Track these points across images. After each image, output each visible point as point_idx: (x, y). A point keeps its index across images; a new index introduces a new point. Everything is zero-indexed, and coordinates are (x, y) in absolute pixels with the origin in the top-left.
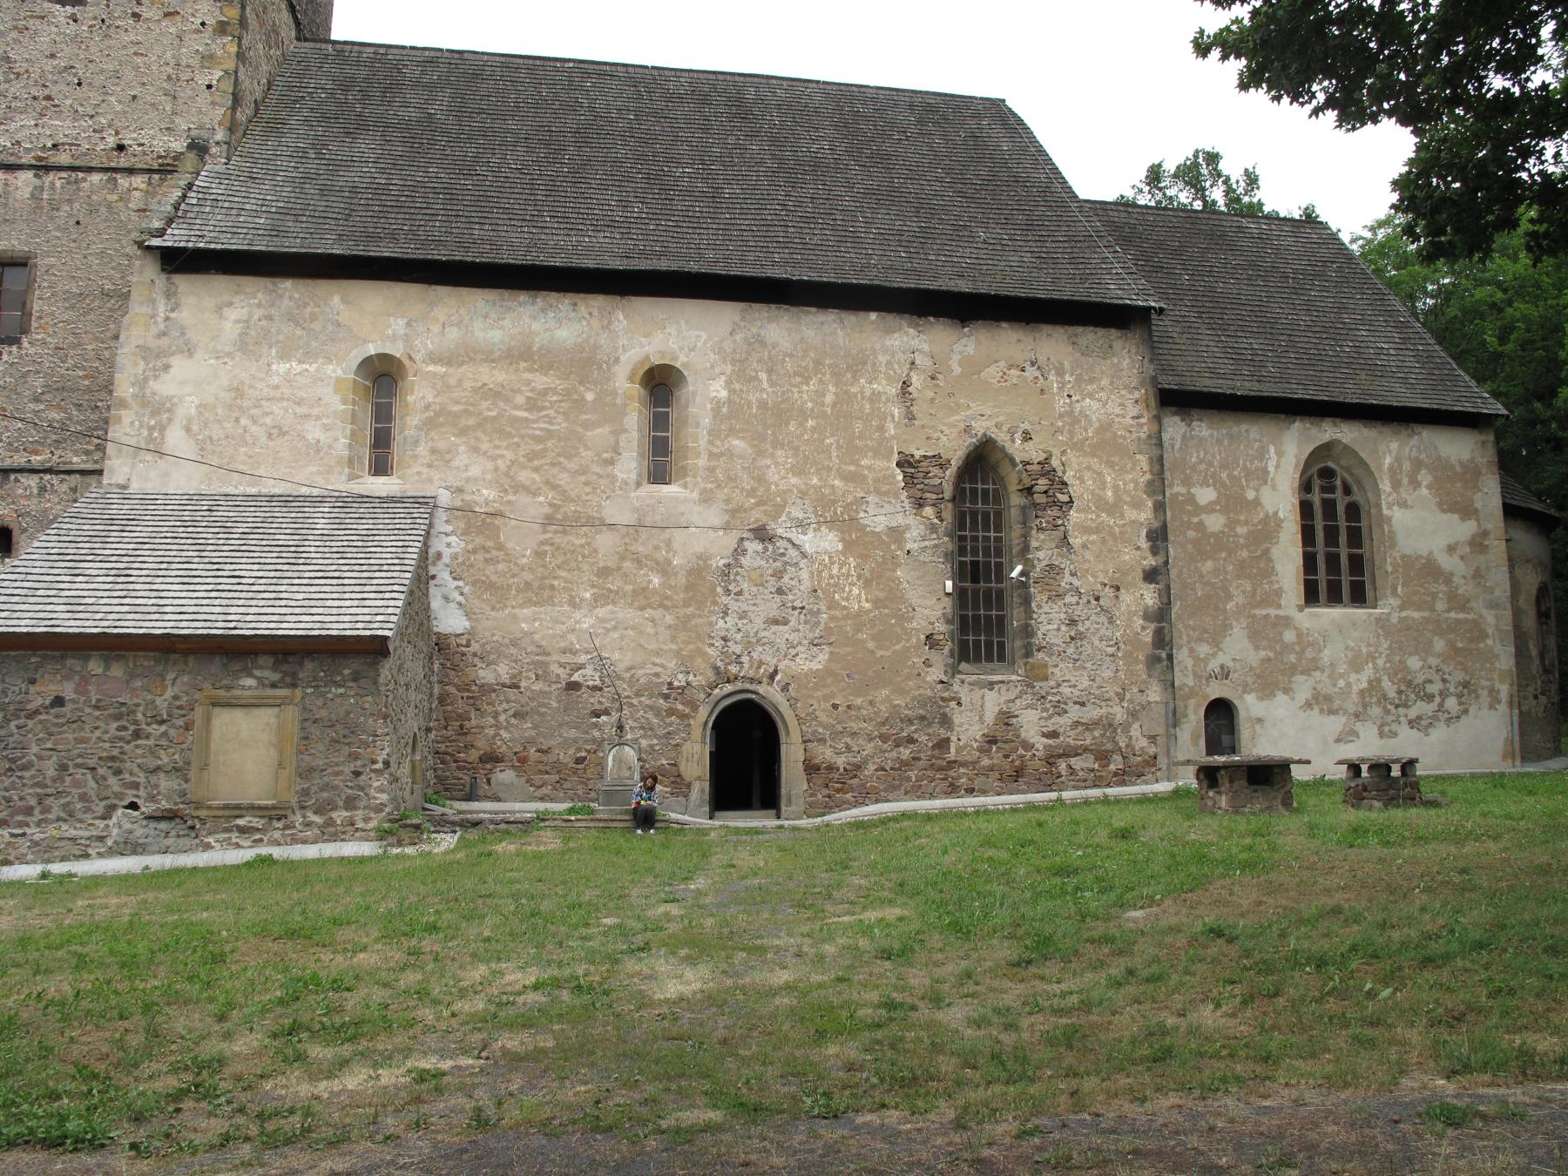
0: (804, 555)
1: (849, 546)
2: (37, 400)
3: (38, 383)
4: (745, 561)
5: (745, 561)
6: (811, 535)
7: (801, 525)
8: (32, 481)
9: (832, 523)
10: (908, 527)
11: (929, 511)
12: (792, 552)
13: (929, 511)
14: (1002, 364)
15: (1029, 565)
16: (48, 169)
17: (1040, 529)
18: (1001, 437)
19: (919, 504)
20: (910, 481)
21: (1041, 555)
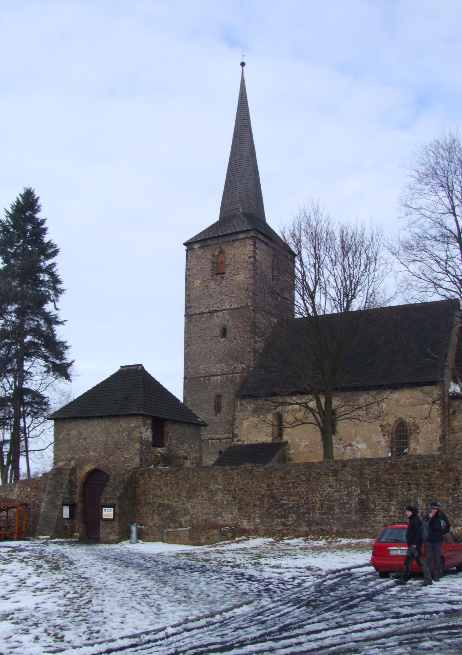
0: (359, 449)
1: (369, 447)
2: (224, 424)
3: (224, 420)
4: (347, 451)
5: (347, 451)
6: (360, 445)
7: (358, 443)
8: (224, 441)
9: (365, 442)
10: (381, 441)
11: (386, 437)
12: (356, 449)
13: (386, 437)
14: (405, 399)
15: (409, 448)
16: (223, 375)
17: (412, 439)
18: (404, 417)
19: (384, 435)
20: (382, 430)
21: (412, 445)
